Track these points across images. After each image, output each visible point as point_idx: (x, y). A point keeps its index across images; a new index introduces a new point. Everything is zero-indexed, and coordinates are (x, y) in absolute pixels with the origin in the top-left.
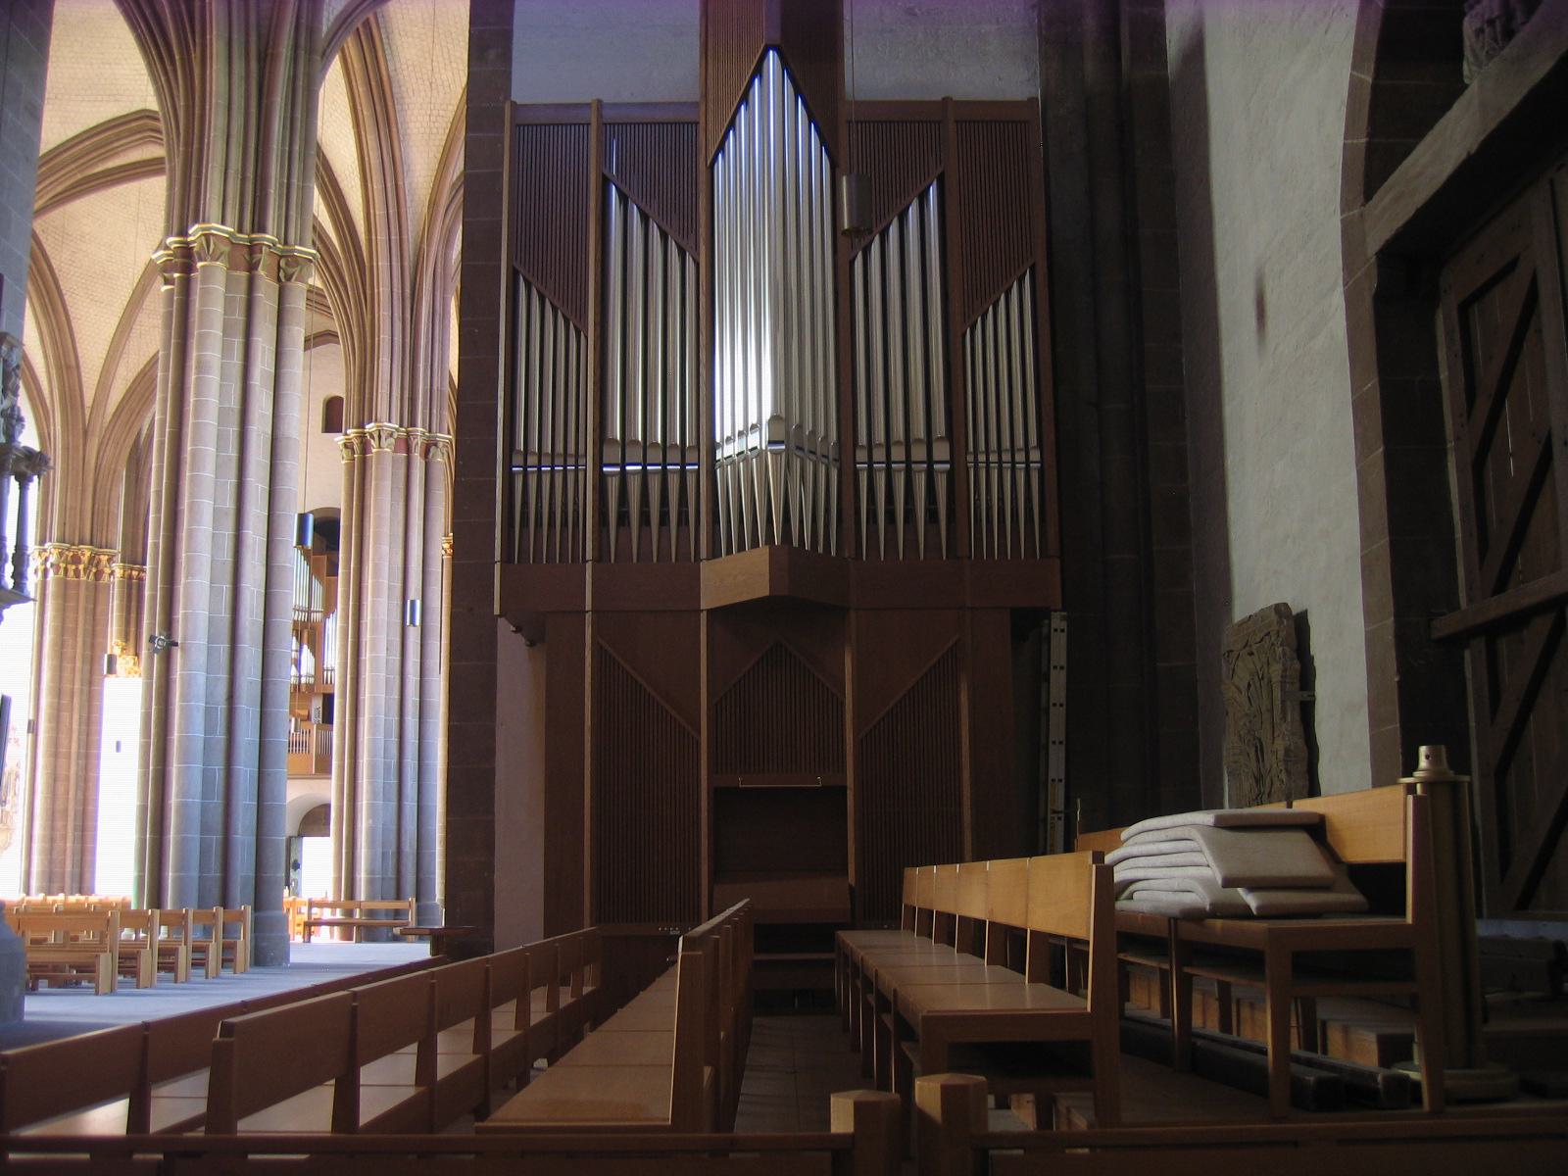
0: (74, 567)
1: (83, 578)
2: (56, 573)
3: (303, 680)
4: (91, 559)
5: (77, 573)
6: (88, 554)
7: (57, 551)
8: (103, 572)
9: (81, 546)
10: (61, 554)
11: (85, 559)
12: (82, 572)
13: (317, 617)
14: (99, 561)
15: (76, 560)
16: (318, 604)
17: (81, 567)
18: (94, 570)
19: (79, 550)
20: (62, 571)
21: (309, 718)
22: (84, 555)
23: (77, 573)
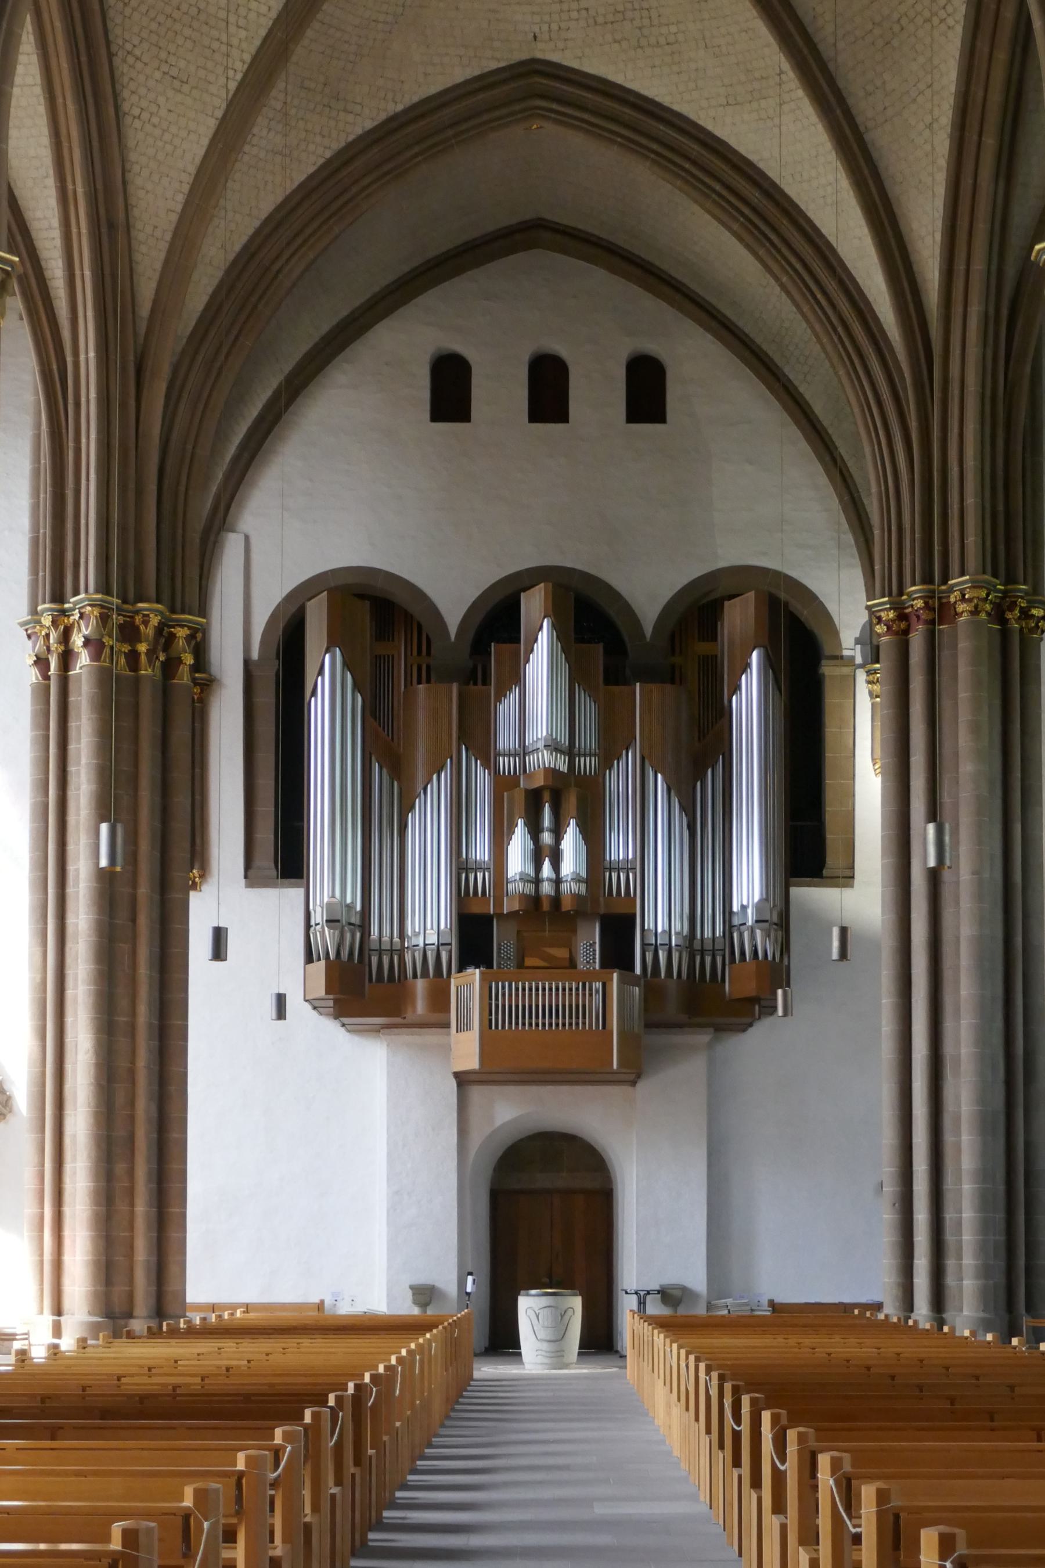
0: (126, 648)
1: (145, 671)
2: (96, 656)
3: (565, 887)
4: (159, 630)
5: (133, 658)
6: (155, 620)
7: (96, 612)
8: (180, 661)
9: (140, 605)
10: (104, 619)
11: (149, 631)
12: (143, 658)
13: (587, 764)
14: (172, 636)
15: (129, 633)
16: (588, 739)
17: (143, 648)
18: (162, 658)
19: (137, 612)
20: (107, 650)
21: (572, 964)
22: (146, 623)
23: (133, 658)
